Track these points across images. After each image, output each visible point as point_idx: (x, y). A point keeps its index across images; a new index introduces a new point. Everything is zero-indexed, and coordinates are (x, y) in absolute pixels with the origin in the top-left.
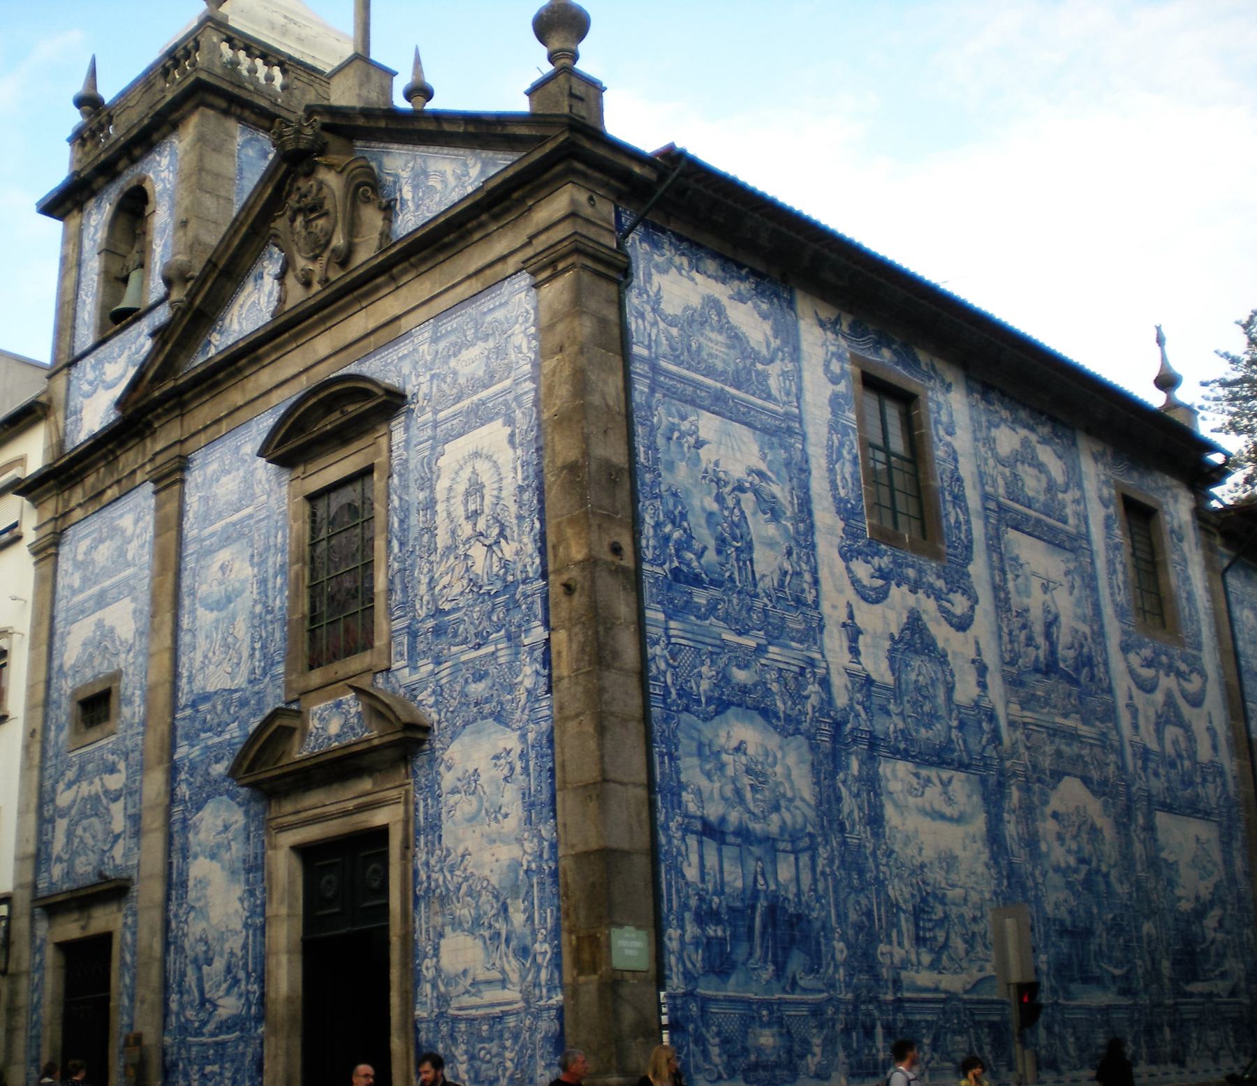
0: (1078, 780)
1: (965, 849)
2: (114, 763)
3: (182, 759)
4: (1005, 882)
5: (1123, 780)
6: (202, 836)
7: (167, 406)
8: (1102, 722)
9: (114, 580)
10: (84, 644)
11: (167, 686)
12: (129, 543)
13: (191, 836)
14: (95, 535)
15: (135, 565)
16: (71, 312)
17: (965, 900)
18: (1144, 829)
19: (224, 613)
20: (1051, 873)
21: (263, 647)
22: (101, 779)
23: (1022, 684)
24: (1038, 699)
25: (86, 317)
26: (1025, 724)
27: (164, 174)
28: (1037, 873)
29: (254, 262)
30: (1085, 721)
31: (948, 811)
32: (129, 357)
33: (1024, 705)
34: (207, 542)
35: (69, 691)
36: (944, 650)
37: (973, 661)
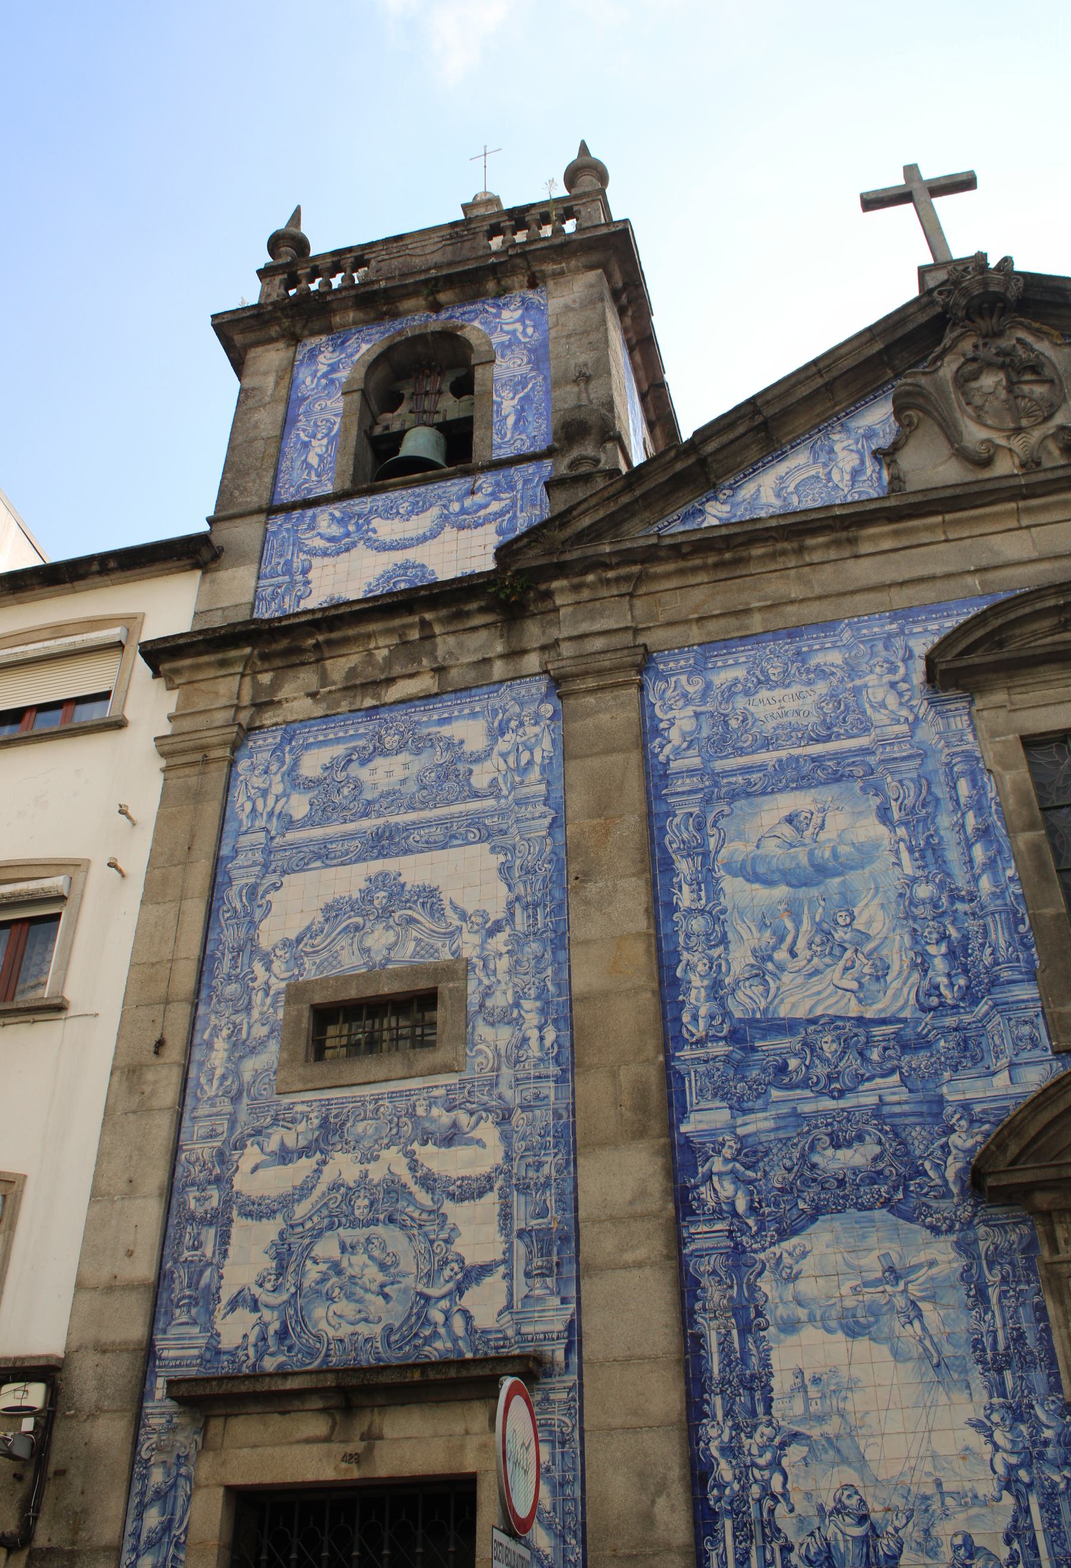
2: (455, 1124)
3: (712, 1133)
6: (805, 1286)
7: (611, 574)
9: (427, 814)
10: (328, 908)
11: (647, 999)
12: (478, 760)
13: (766, 1285)
14: (361, 743)
15: (498, 797)
16: (272, 450)
19: (814, 892)
21: (951, 955)
22: (410, 1155)
25: (314, 460)
27: (506, 328)
29: (808, 431)
32: (444, 519)
34: (740, 779)
35: (279, 985)
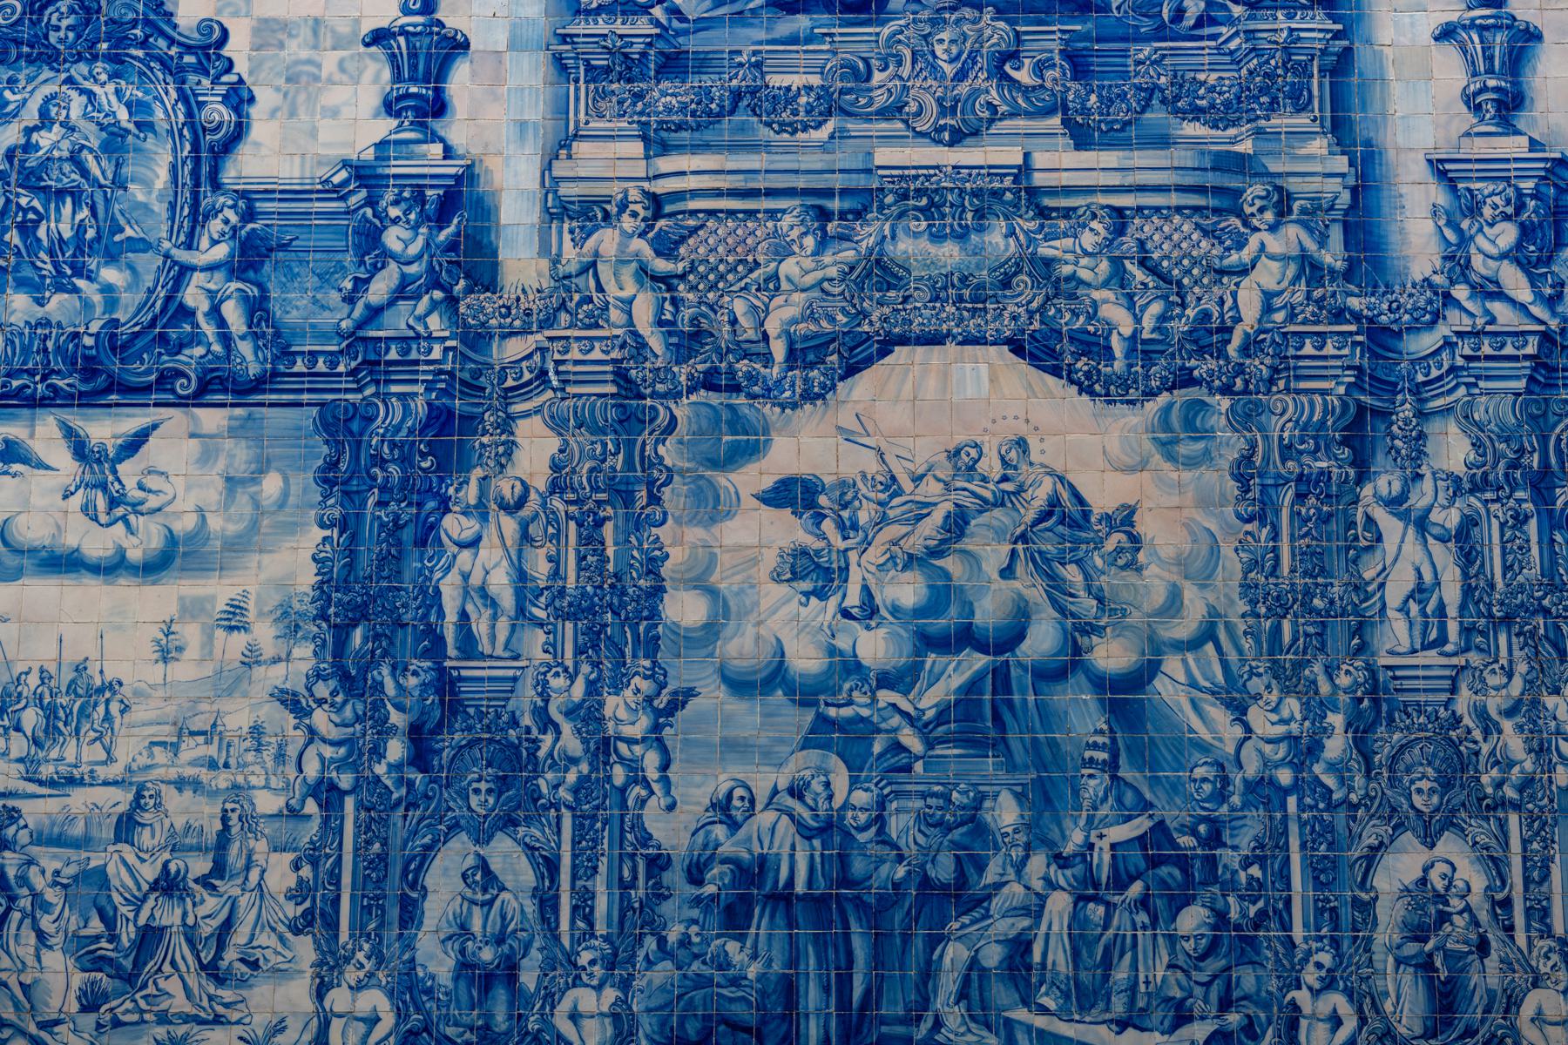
0: (1000, 355)
1: (166, 655)
4: (396, 750)
5: (1339, 315)
8: (1221, 116)
17: (126, 827)
18: (1457, 486)
20: (712, 697)
23: (673, 64)
24: (788, 97)
26: (656, 203)
28: (614, 705)
30: (1082, 138)
31: (97, 543)
33: (657, 142)
36: (205, 26)
37: (378, 37)
